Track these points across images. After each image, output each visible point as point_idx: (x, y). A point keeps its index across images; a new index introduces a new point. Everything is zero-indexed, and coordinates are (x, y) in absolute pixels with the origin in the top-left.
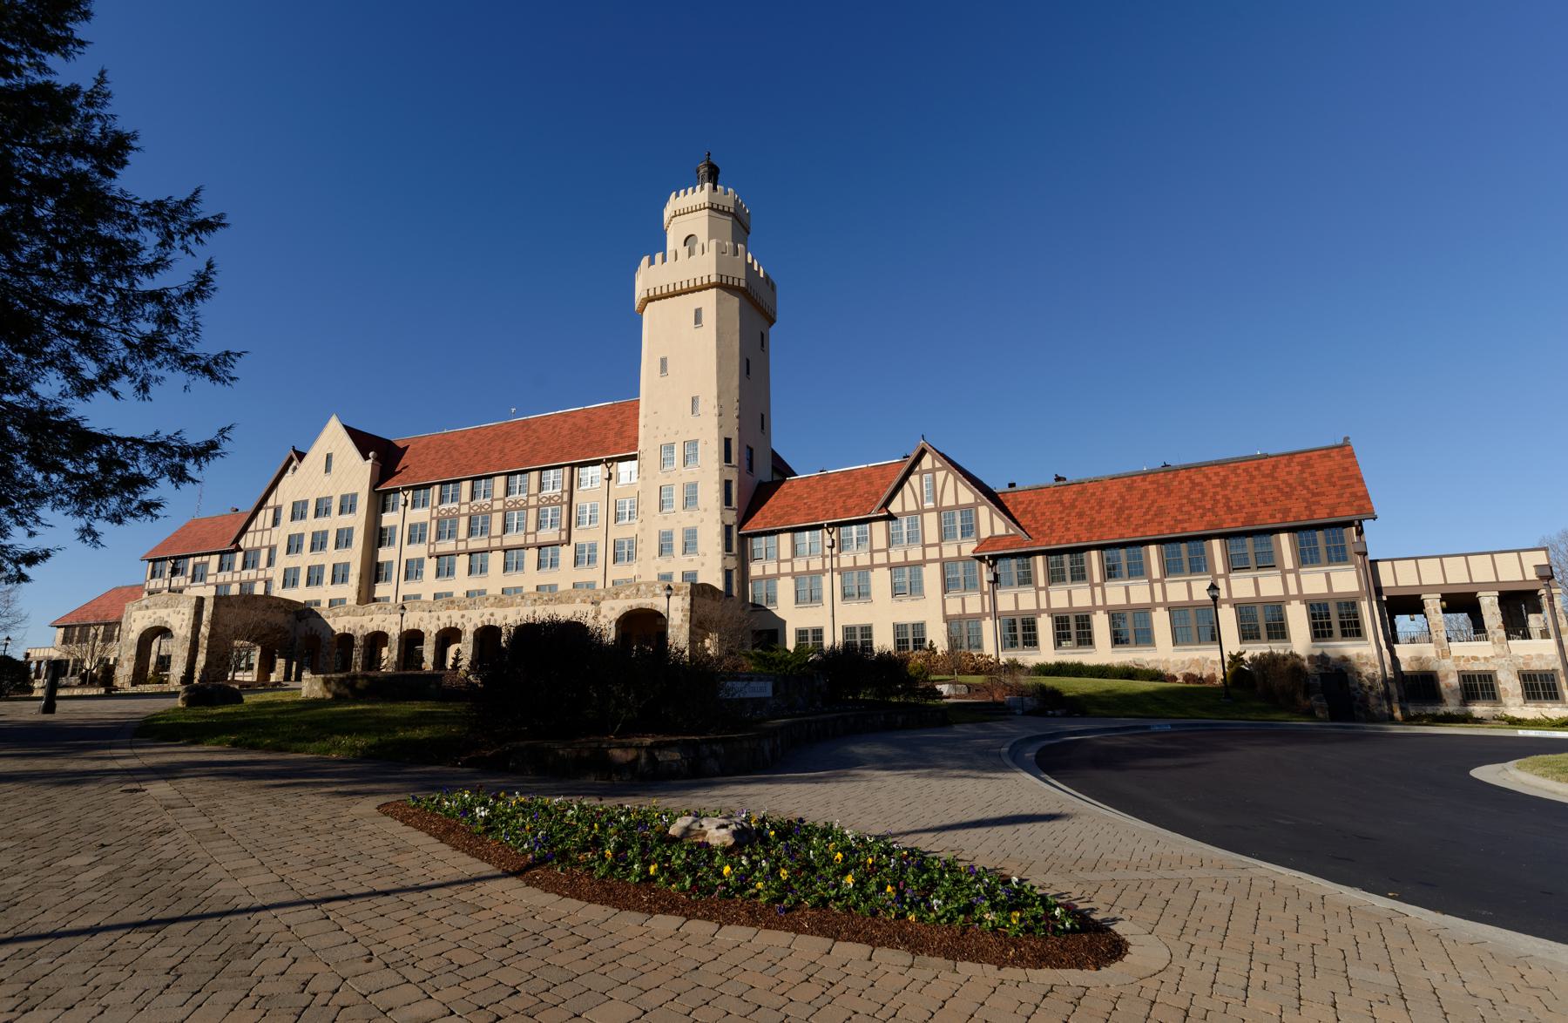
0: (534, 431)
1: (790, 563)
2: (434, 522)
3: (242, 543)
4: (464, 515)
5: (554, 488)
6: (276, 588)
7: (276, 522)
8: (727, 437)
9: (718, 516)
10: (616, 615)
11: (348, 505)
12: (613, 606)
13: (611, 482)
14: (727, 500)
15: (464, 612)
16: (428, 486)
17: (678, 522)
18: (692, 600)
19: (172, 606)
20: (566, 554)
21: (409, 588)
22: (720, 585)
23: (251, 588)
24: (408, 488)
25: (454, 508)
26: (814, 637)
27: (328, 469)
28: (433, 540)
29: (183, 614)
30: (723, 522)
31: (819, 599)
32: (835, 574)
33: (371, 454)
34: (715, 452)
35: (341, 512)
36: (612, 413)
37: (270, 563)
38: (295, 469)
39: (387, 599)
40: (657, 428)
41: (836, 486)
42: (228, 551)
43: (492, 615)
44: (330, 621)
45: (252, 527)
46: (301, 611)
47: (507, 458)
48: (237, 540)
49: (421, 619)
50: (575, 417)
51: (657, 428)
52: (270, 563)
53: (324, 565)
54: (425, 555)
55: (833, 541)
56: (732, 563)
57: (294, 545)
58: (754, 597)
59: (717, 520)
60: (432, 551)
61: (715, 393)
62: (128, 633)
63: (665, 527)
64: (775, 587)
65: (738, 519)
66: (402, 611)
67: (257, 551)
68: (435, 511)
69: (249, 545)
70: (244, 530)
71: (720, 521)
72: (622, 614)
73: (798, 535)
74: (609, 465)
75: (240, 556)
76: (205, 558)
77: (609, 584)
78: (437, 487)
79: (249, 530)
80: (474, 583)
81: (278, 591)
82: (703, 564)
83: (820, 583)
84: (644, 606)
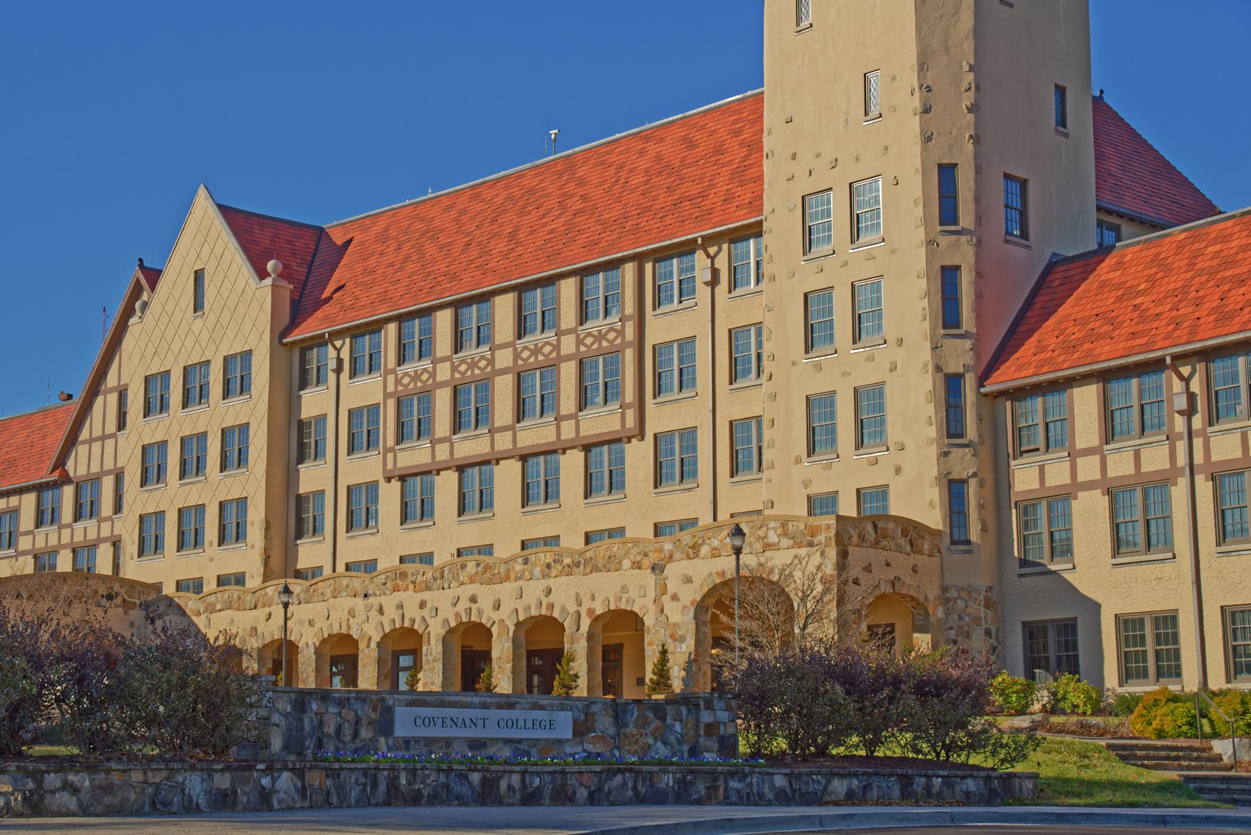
0: (582, 182)
1: (1097, 458)
2: (391, 403)
3: (70, 466)
4: (504, 371)
5: (606, 314)
6: (128, 555)
7: (121, 425)
8: (946, 161)
9: (927, 355)
10: (691, 595)
11: (236, 383)
12: (690, 573)
13: (717, 289)
14: (949, 316)
15: (425, 595)
16: (375, 328)
17: (844, 374)
18: (843, 554)
20: (638, 457)
21: (355, 548)
22: (934, 519)
23: (92, 557)
25: (425, 370)
26: (1158, 636)
27: (198, 306)
30: (938, 369)
31: (1168, 544)
32: (1199, 479)
33: (270, 265)
34: (916, 203)
35: (226, 394)
36: (736, 122)
37: (118, 508)
38: (145, 305)
39: (316, 571)
40: (794, 157)
41: (1216, 255)
42: (47, 483)
43: (473, 599)
44: (200, 622)
45: (84, 435)
46: (153, 602)
47: (520, 250)
48: (60, 463)
49: (352, 613)
50: (661, 140)
51: (794, 157)
52: (118, 508)
53: (203, 505)
54: (378, 475)
55: (1191, 397)
56: (963, 464)
57: (152, 473)
58: (1024, 541)
59: (925, 366)
61: (912, 58)
63: (818, 386)
64: (1068, 516)
65: (978, 357)
66: (285, 598)
67: (96, 480)
68: (391, 378)
69: (82, 471)
70: (71, 441)
71: (930, 367)
72: (705, 590)
73: (1116, 387)
74: (712, 250)
76: (14, 501)
78: (392, 327)
79: (80, 439)
80: (471, 532)
81: (136, 569)
82: (898, 470)
83: (1166, 502)
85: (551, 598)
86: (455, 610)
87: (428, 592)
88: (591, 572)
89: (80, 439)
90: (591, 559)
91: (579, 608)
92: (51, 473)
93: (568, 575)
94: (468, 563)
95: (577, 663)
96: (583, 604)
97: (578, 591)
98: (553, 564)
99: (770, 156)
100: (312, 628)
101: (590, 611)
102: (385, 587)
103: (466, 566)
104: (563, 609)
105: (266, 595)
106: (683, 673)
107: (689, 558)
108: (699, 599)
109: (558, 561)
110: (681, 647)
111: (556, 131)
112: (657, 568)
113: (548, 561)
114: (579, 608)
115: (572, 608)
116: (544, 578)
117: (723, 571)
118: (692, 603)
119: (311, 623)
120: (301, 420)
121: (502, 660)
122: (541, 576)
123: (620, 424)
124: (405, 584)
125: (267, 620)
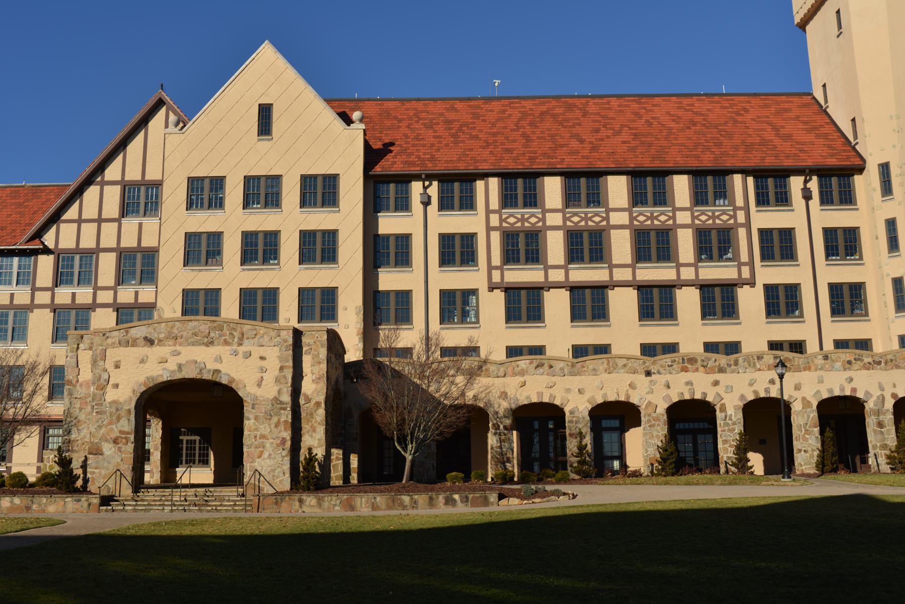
2: (496, 237)
3: (49, 239)
13: (810, 202)
15: (718, 376)
19: (226, 343)
24: (430, 177)
28: (496, 260)
29: (262, 358)
45: (72, 213)
48: (38, 235)
49: (632, 386)
60: (496, 277)
62: (103, 388)
67: (90, 256)
70: (55, 218)
75: (45, 265)
77: (829, 346)
79: (64, 217)
85: (853, 385)
86: (753, 388)
87: (721, 374)
88: (892, 369)
89: (64, 218)
90: (892, 360)
91: (882, 393)
92: (28, 242)
93: (869, 370)
94: (765, 356)
95: (885, 429)
100: (581, 396)
101: (894, 395)
102: (671, 368)
103: (762, 357)
104: (867, 393)
105: (518, 366)
109: (859, 359)
111: (499, 81)
113: (848, 359)
114: (882, 393)
115: (876, 393)
116: (845, 370)
119: (580, 391)
120: (378, 235)
121: (808, 425)
123: (737, 275)
124: (694, 367)
125: (521, 387)
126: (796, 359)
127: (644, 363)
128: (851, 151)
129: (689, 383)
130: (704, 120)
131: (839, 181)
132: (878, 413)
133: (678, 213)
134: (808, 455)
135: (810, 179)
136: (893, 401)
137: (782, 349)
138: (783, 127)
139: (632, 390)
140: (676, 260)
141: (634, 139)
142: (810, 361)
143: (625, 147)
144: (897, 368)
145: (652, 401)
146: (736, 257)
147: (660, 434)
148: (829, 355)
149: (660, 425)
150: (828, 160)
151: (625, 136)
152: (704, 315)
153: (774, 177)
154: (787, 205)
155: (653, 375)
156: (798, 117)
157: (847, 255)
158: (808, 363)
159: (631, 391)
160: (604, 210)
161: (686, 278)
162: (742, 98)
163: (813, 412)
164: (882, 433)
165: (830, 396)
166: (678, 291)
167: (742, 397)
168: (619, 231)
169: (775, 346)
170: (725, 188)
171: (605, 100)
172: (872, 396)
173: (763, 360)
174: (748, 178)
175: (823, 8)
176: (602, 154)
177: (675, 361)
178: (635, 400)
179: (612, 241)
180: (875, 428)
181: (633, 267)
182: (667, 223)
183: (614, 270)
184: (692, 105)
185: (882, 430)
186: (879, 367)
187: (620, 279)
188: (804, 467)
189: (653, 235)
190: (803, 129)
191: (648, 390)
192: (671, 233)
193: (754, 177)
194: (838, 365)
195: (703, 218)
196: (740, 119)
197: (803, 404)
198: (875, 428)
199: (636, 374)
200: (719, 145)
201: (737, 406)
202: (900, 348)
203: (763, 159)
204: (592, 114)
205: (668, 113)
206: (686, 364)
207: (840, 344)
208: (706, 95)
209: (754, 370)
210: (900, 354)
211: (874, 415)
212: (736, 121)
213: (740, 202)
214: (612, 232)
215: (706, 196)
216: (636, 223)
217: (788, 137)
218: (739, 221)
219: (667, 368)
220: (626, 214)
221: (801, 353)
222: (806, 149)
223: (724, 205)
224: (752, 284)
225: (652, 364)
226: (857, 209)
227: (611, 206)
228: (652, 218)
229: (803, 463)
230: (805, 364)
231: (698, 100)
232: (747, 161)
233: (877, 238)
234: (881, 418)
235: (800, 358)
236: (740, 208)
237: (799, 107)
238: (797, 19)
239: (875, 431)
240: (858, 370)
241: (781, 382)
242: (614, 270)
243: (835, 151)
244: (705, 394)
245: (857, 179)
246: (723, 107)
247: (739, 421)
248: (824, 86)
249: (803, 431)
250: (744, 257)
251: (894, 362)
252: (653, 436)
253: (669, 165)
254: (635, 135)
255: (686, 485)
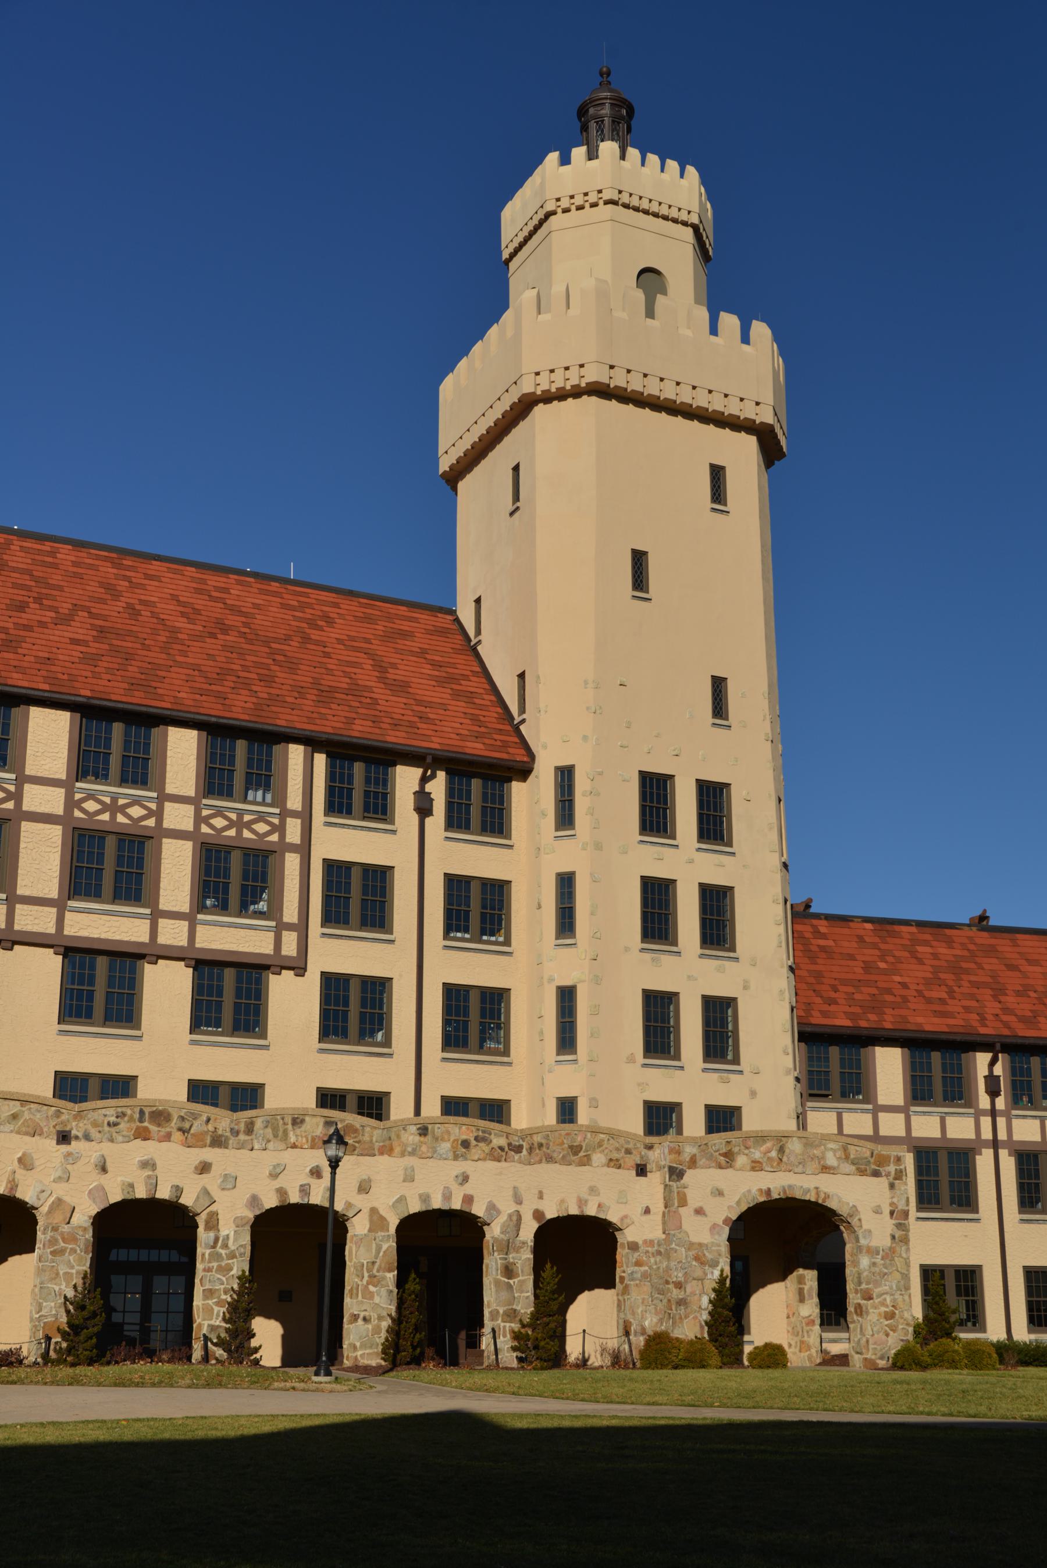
12: (722, 1185)
13: (428, 821)
15: (209, 1154)
32: (1003, 1153)
49: (25, 1163)
59: (781, 992)
72: (744, 1208)
77: (432, 1108)
84: (798, 1195)
85: (469, 1189)
87: (217, 1150)
88: (540, 1162)
90: (540, 1145)
94: (307, 1119)
95: (516, 1280)
96: (524, 1202)
97: (517, 1185)
98: (473, 1143)
99: (598, 712)
101: (538, 1214)
102: (113, 1130)
103: (303, 1121)
104: (492, 1207)
106: (710, 1307)
107: (721, 1167)
108: (734, 1218)
110: (712, 1273)
112: (676, 1173)
113: (464, 1137)
114: (518, 1207)
115: (507, 1207)
116: (456, 1158)
117: (769, 1189)
118: (725, 1222)
121: (376, 1266)
122: (451, 1155)
123: (272, 947)
124: (164, 1131)
126: (368, 1129)
127: (58, 1114)
128: (512, 733)
129: (148, 1164)
130: (246, 625)
131: (485, 787)
132: (507, 1247)
133: (168, 806)
134: (370, 1327)
135: (433, 776)
136: (535, 1226)
137: (342, 1107)
138: (394, 666)
139: (24, 1172)
140: (153, 902)
141: (96, 640)
142: (393, 1136)
143: (76, 652)
144: (548, 1162)
145: (65, 1198)
146: (274, 912)
147: (74, 1271)
148: (430, 1127)
149: (75, 1251)
150: (469, 744)
151: (80, 628)
152: (196, 1025)
153: (367, 761)
154: (384, 821)
155: (73, 1143)
156: (423, 652)
157: (483, 932)
158: (390, 1139)
159: (21, 1174)
160: (13, 776)
161: (169, 942)
162: (324, 596)
163: (388, 1240)
164: (510, 1287)
165: (424, 1209)
166: (148, 968)
167: (254, 1200)
168: (41, 826)
169: (329, 1099)
170: (269, 769)
171: (47, 546)
172: (499, 1212)
173: (304, 1127)
174: (316, 755)
175: (491, 455)
176: (27, 658)
177: (124, 1114)
178: (27, 1194)
179: (22, 845)
180: (499, 1277)
181: (60, 906)
182: (143, 823)
183: (19, 908)
184: (226, 591)
185: (511, 1282)
186: (517, 1157)
187: (29, 928)
188: (359, 1353)
189: (111, 843)
190: (431, 677)
191: (59, 1173)
192: (148, 845)
193: (330, 755)
194: (445, 1147)
195: (219, 822)
196: (315, 635)
197: (371, 1221)
198: (499, 1277)
199: (37, 1137)
200: (268, 680)
201: (242, 1218)
202: (558, 1122)
203: (350, 721)
204: (15, 570)
205: (175, 598)
206: (146, 1124)
207: (453, 1106)
208: (255, 575)
209: (283, 1146)
210: (557, 1133)
211: (500, 1251)
212: (306, 639)
213: (294, 801)
214: (25, 826)
215: (231, 779)
216: (77, 814)
217: (402, 687)
218: (289, 839)
219: (106, 1128)
220: (60, 793)
221: (379, 1117)
222: (431, 716)
223: (263, 803)
224: (300, 970)
225: (75, 1117)
226: (511, 847)
227: (29, 771)
228: (114, 808)
229: (358, 1344)
230: (384, 1141)
231: (239, 583)
232: (318, 721)
233: (539, 907)
234: (511, 1257)
235: (375, 1128)
236: (294, 814)
237: (428, 632)
238: (445, 464)
239: (497, 1283)
240: (479, 1159)
241: (333, 1174)
242: (19, 908)
243: (483, 729)
244: (178, 1190)
245: (517, 789)
246: (284, 606)
247: (242, 1250)
248: (478, 601)
249: (366, 1278)
250: (290, 913)
251: (544, 1149)
252: (57, 1274)
253: (163, 704)
254: (101, 630)
255: (116, 1385)
